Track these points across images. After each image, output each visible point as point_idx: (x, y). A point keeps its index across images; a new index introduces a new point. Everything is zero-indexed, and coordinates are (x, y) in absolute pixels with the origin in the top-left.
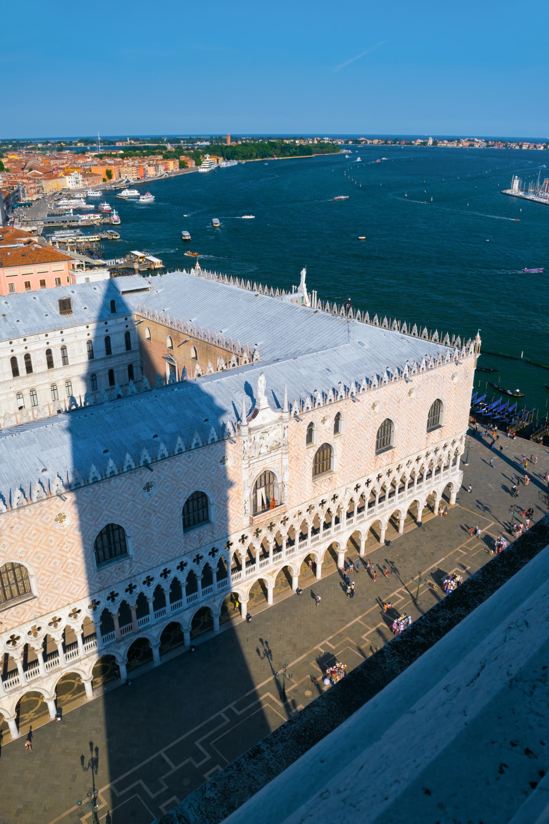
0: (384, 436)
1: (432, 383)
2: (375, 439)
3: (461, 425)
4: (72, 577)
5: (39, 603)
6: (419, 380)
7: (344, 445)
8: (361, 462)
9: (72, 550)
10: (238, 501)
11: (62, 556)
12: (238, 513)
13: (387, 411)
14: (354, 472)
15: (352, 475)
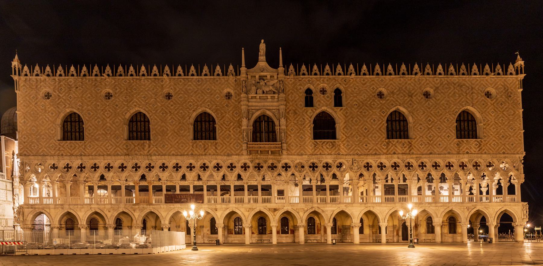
3: (512, 147)
4: (108, 136)
5: (85, 146)
9: (111, 118)
10: (239, 129)
11: (104, 119)
12: (239, 139)
13: (397, 101)
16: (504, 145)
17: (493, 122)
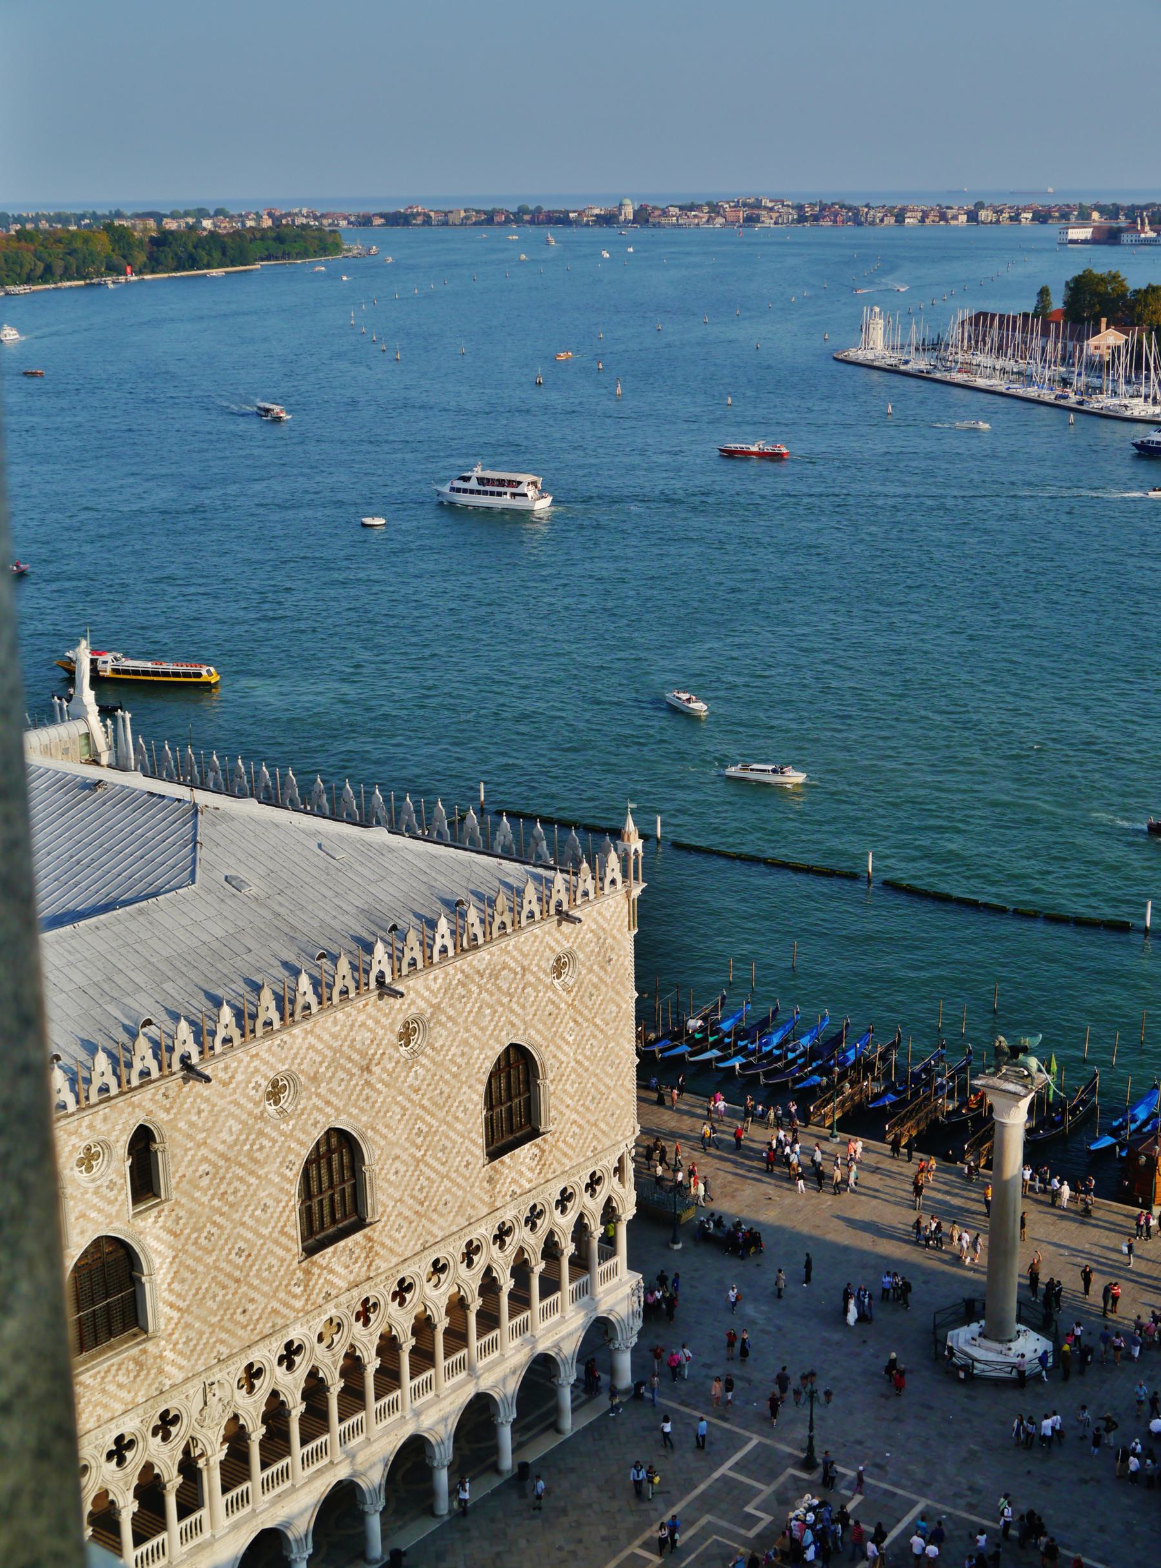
0: (331, 1186)
1: (484, 995)
2: (295, 1202)
3: (612, 1121)
6: (435, 987)
7: (176, 1235)
8: (251, 1286)
13: (328, 1103)
14: (230, 1326)
15: (224, 1336)
16: (596, 1125)
17: (573, 1064)
